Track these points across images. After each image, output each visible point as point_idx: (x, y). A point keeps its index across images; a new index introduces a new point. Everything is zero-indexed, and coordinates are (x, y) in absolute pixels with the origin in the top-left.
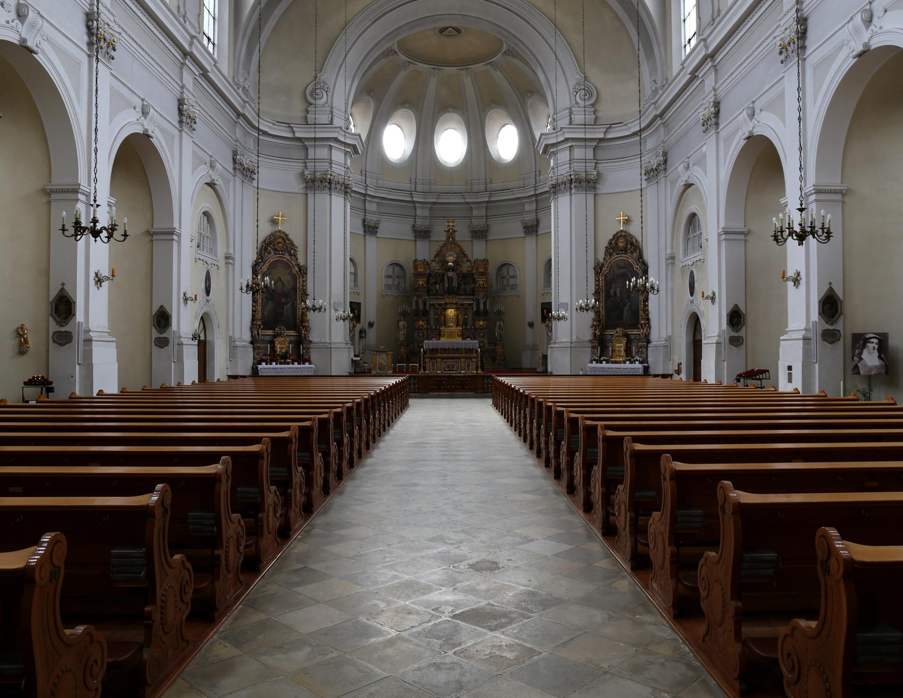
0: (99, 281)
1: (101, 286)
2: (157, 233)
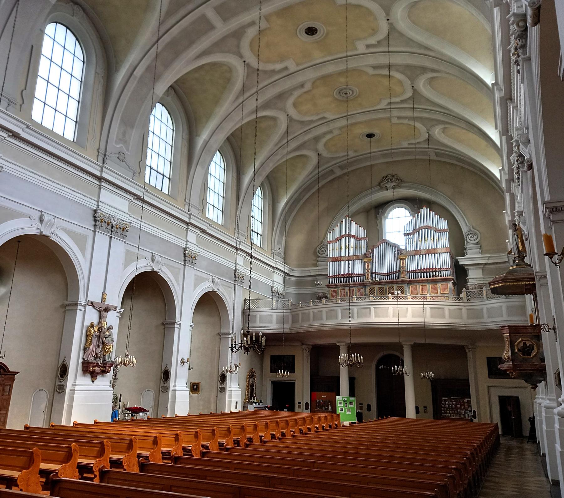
0: (183, 362)
1: (183, 364)
2: (222, 334)
